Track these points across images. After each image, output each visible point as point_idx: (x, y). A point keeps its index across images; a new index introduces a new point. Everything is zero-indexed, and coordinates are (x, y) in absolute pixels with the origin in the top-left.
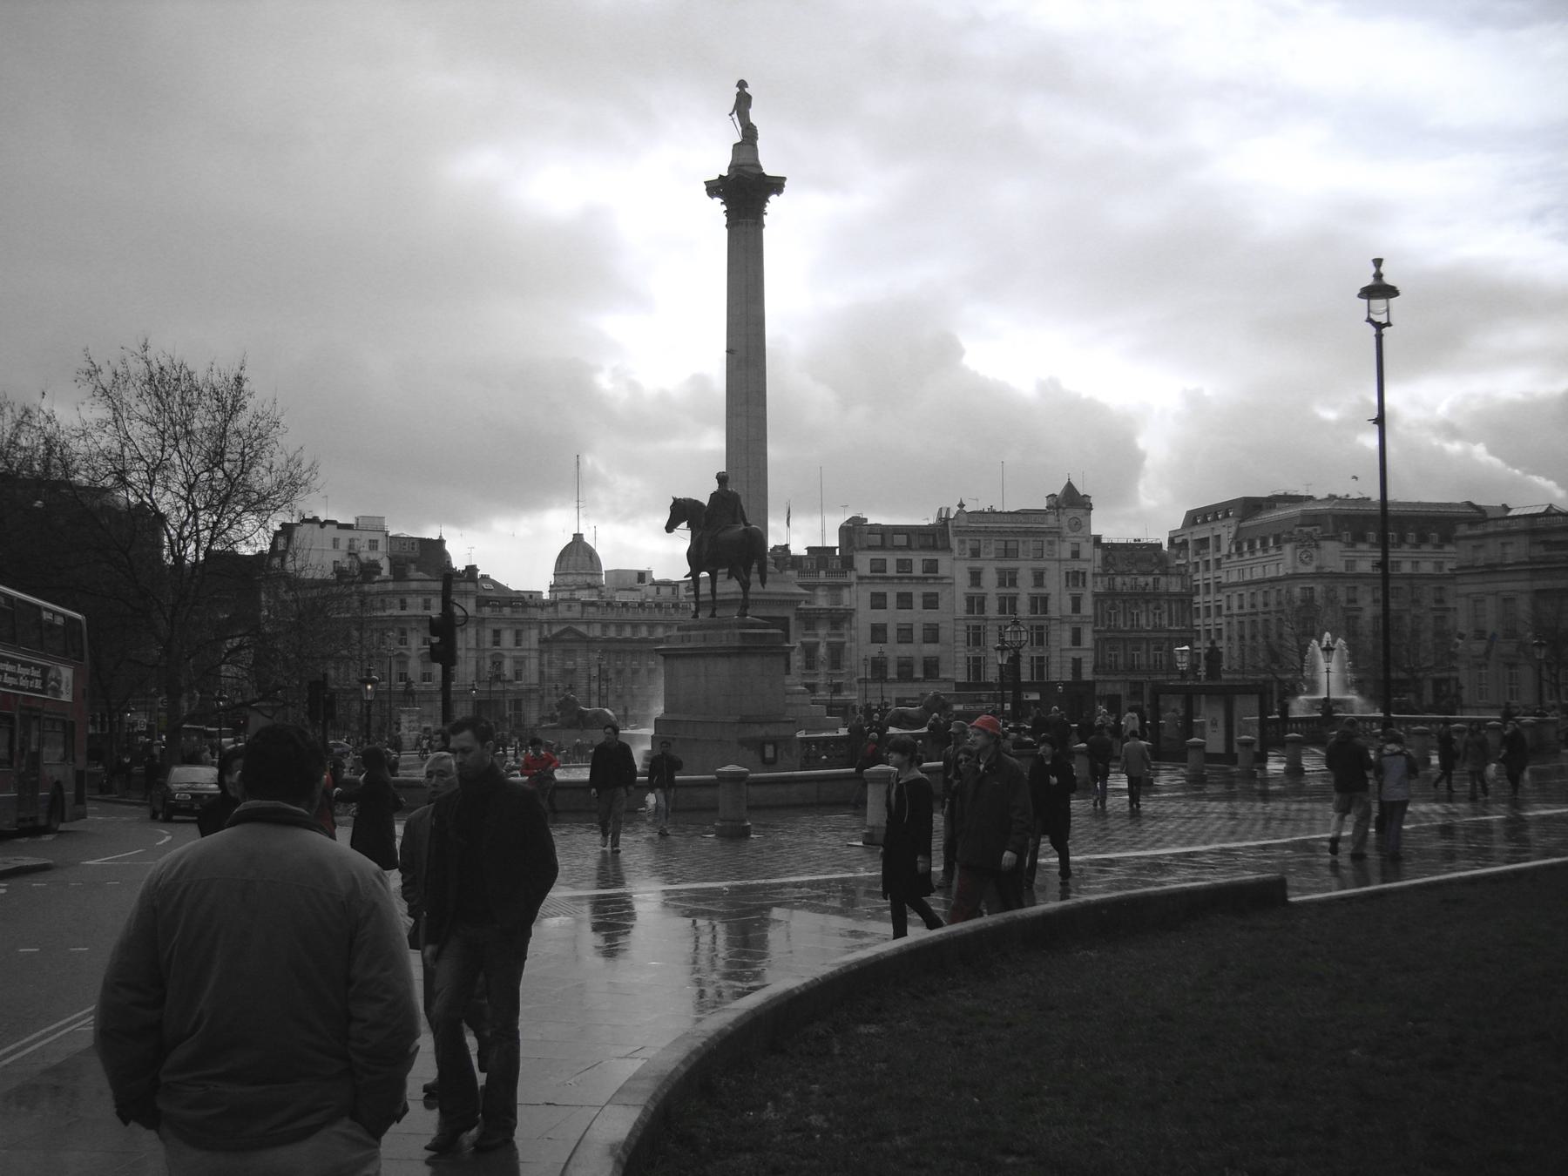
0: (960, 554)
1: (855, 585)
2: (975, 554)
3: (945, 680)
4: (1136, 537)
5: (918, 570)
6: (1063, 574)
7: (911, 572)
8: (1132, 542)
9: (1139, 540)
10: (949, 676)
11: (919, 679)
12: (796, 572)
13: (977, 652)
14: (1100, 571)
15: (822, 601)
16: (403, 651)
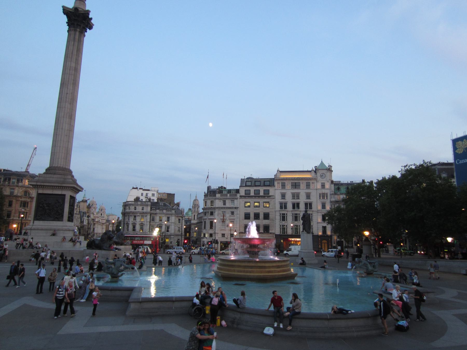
0: (277, 187)
1: (239, 199)
2: (283, 186)
3: (271, 233)
4: (352, 180)
5: (262, 193)
6: (318, 194)
7: (259, 194)
8: (350, 182)
9: (353, 182)
10: (273, 232)
11: (262, 232)
12: (220, 195)
13: (283, 223)
14: (333, 193)
15: (228, 204)
16: (128, 222)
